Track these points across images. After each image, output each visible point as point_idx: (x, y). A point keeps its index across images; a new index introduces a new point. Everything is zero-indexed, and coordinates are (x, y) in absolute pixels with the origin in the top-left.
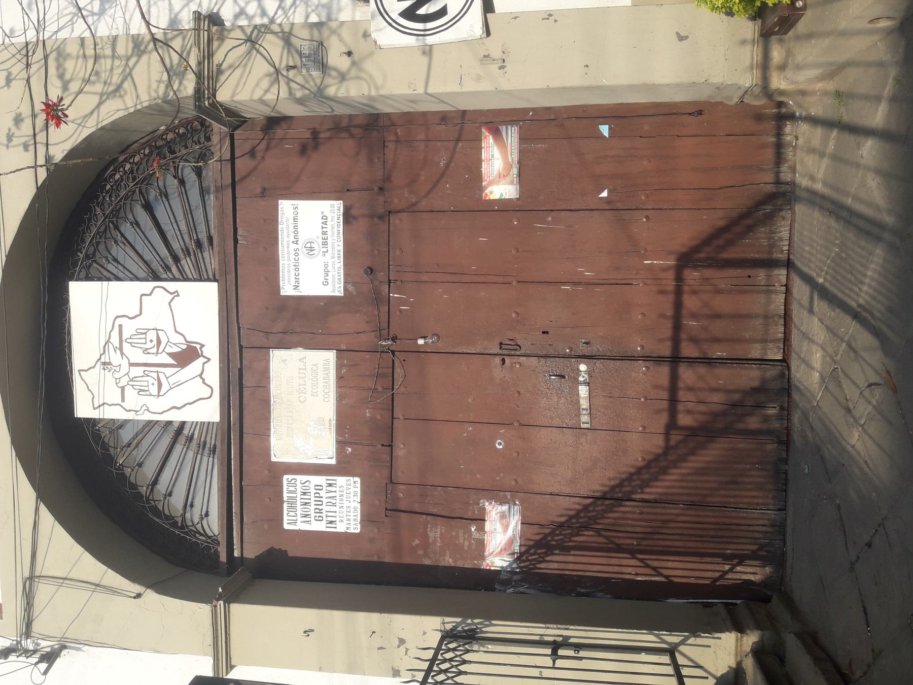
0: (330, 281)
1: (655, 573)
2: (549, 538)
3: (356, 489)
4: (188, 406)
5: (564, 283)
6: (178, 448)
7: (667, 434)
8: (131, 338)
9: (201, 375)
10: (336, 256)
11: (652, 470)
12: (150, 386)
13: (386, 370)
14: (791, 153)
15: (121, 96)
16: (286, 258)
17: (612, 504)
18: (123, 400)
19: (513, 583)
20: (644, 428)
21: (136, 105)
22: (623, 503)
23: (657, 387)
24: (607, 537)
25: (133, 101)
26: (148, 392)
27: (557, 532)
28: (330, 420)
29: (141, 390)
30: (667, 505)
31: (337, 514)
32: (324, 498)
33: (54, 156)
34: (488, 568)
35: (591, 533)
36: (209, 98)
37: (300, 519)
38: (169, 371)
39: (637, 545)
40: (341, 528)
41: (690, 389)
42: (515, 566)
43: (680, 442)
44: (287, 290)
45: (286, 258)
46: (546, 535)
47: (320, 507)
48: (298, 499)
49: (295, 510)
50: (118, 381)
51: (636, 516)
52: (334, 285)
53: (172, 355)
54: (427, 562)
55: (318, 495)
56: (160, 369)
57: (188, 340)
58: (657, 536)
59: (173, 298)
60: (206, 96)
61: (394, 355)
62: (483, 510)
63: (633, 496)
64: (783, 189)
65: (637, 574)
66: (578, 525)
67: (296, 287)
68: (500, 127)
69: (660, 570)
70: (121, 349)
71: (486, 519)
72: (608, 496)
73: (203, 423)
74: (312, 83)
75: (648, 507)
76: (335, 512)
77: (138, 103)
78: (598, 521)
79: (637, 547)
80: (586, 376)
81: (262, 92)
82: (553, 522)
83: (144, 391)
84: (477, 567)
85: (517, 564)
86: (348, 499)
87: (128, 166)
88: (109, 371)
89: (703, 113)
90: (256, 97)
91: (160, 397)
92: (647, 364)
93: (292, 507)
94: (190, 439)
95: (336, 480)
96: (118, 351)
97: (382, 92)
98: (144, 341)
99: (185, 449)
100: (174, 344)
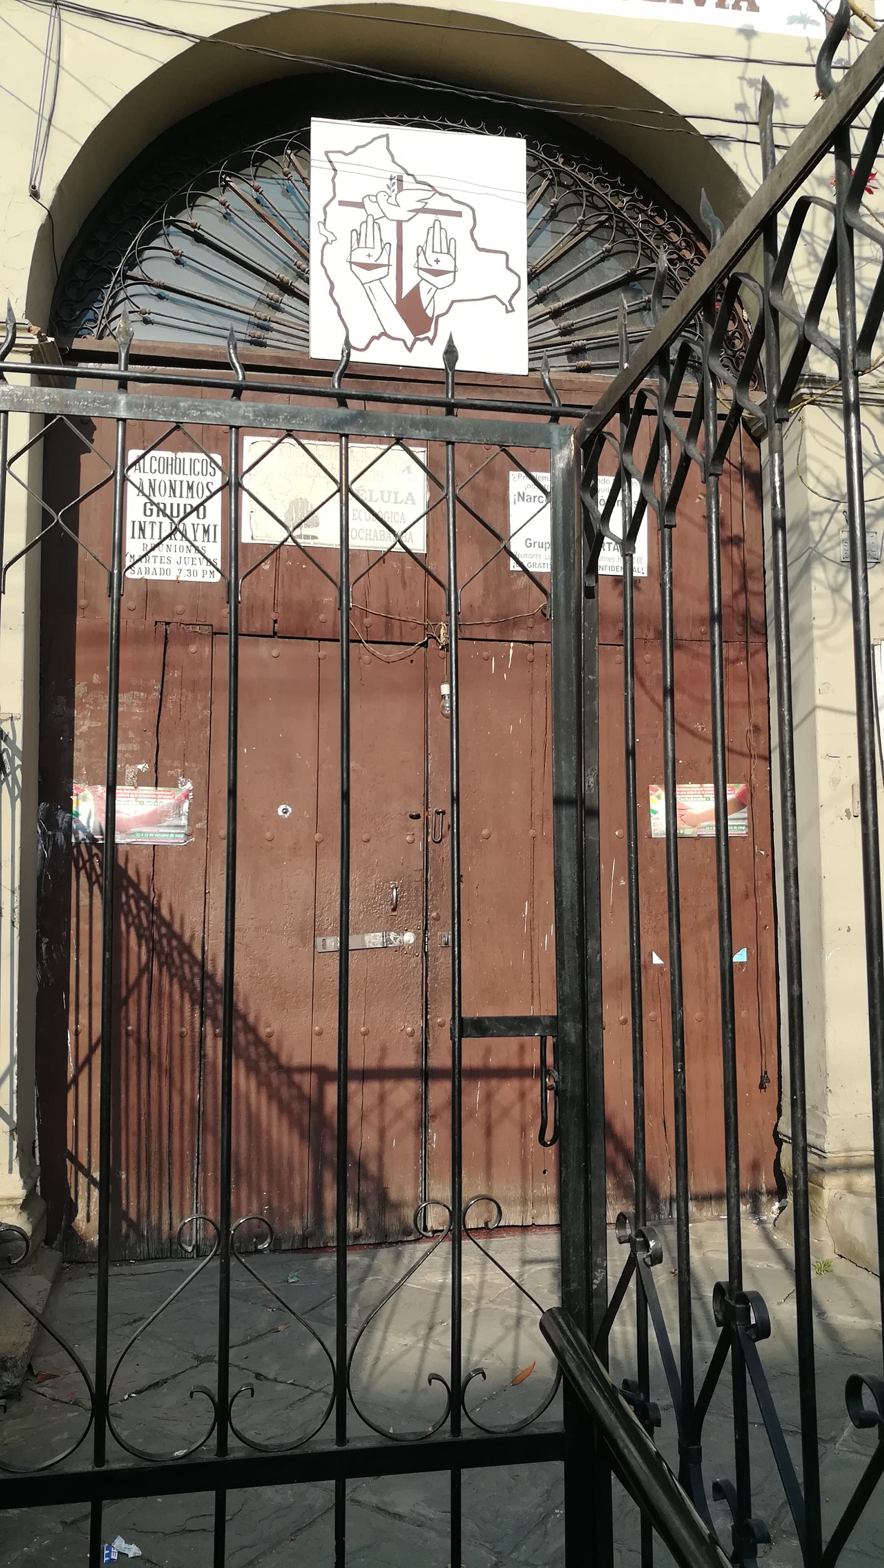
0: (532, 551)
1: (80, 1061)
2: (131, 891)
3: (200, 574)
4: (336, 308)
5: (531, 906)
6: (259, 284)
7: (310, 1069)
8: (441, 228)
9: (384, 334)
11: (252, 1049)
12: (368, 251)
13: (396, 631)
14: (709, 1214)
15: (809, 263)
17: (195, 989)
18: (342, 203)
19: (50, 833)
20: (320, 1034)
21: (798, 285)
22: (198, 1007)
23: (384, 1050)
24: (138, 983)
25: (806, 280)
26: (355, 246)
27: (142, 904)
28: (314, 537)
29: (359, 235)
30: (197, 1074)
33: (729, 149)
34: (75, 792)
35: (144, 958)
36: (812, 394)
38: (391, 283)
39: (127, 1030)
41: (382, 1098)
42: (81, 835)
43: (299, 1088)
46: (136, 887)
48: (181, 477)
49: (161, 471)
50: (373, 199)
51: (177, 1029)
53: (416, 289)
54: (80, 689)
56: (393, 270)
57: (440, 319)
58: (144, 1061)
59: (503, 304)
60: (814, 391)
61: (421, 645)
62: (173, 783)
63: (208, 1023)
64: (663, 1207)
65: (77, 1033)
66: (156, 936)
68: (745, 810)
69: (86, 1071)
70: (424, 210)
71: (159, 788)
72: (207, 983)
73: (308, 328)
74: (828, 545)
75: (193, 1047)
77: (801, 288)
78: (165, 969)
79: (123, 1032)
80: (397, 943)
81: (816, 473)
82: (160, 897)
83: (358, 240)
84: (75, 772)
85: (84, 839)
86: (183, 559)
87: (689, 256)
88: (388, 186)
89: (763, 1090)
90: (810, 463)
91: (348, 264)
92: (418, 1033)
93: (168, 467)
94: (275, 307)
95: (215, 541)
96: (420, 205)
97: (817, 646)
98: (437, 249)
99: (258, 295)
100: (433, 297)
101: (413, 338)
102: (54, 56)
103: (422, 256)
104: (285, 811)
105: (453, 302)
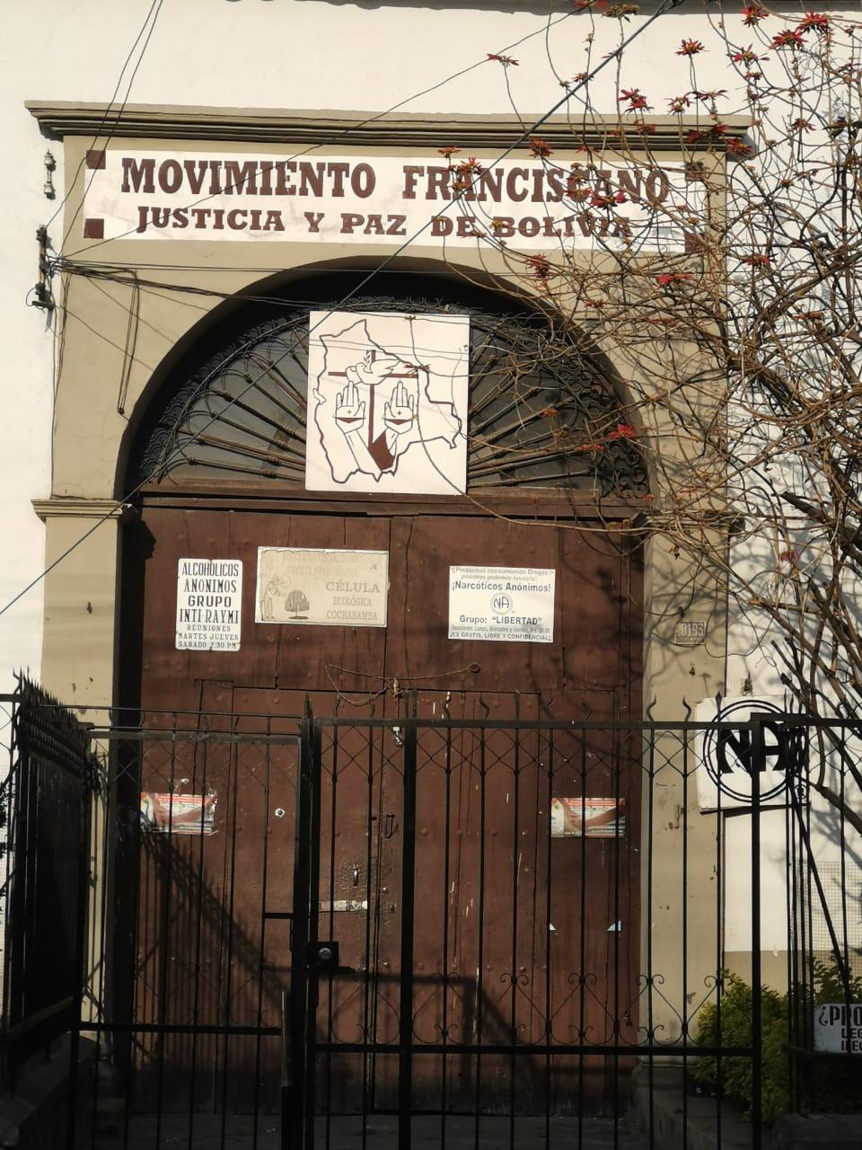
0: (465, 624)
10: (493, 632)
12: (347, 409)
13: (363, 684)
16: (491, 574)
18: (330, 374)
28: (306, 618)
31: (196, 623)
32: (216, 608)
37: (190, 578)
40: (181, 627)
44: (456, 574)
45: (491, 574)
47: (205, 603)
48: (215, 577)
52: (460, 628)
53: (383, 437)
55: (219, 601)
59: (448, 442)
67: (458, 584)
70: (391, 375)
76: (199, 621)
80: (357, 908)
83: (342, 401)
93: (204, 570)
95: (237, 622)
96: (388, 372)
98: (400, 404)
101: (380, 472)
102: (135, 312)
103: (388, 409)
104: (280, 813)
105: (411, 443)
